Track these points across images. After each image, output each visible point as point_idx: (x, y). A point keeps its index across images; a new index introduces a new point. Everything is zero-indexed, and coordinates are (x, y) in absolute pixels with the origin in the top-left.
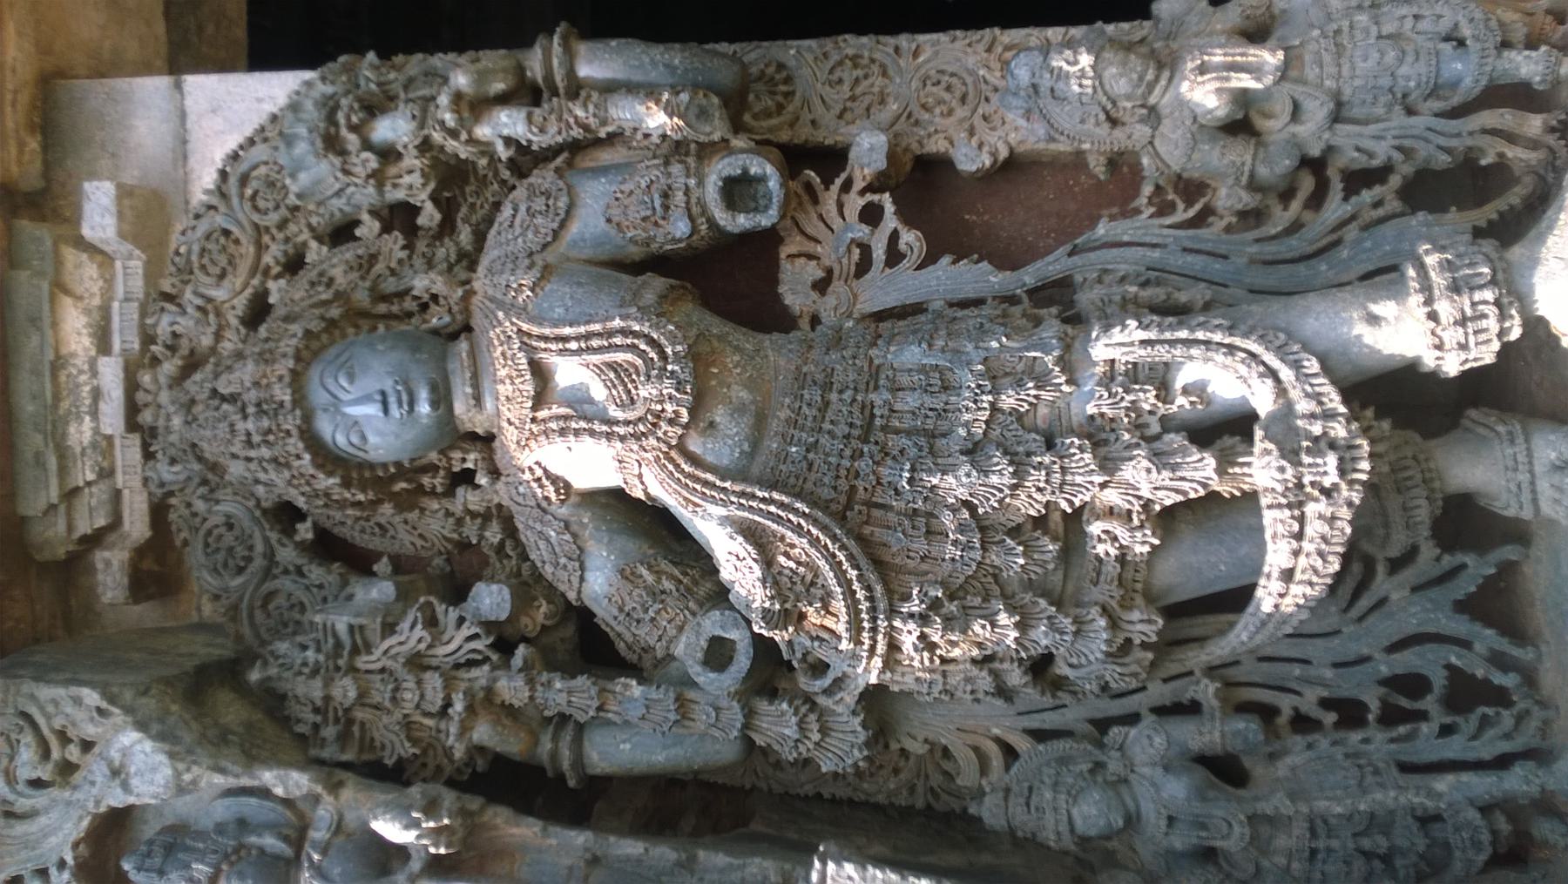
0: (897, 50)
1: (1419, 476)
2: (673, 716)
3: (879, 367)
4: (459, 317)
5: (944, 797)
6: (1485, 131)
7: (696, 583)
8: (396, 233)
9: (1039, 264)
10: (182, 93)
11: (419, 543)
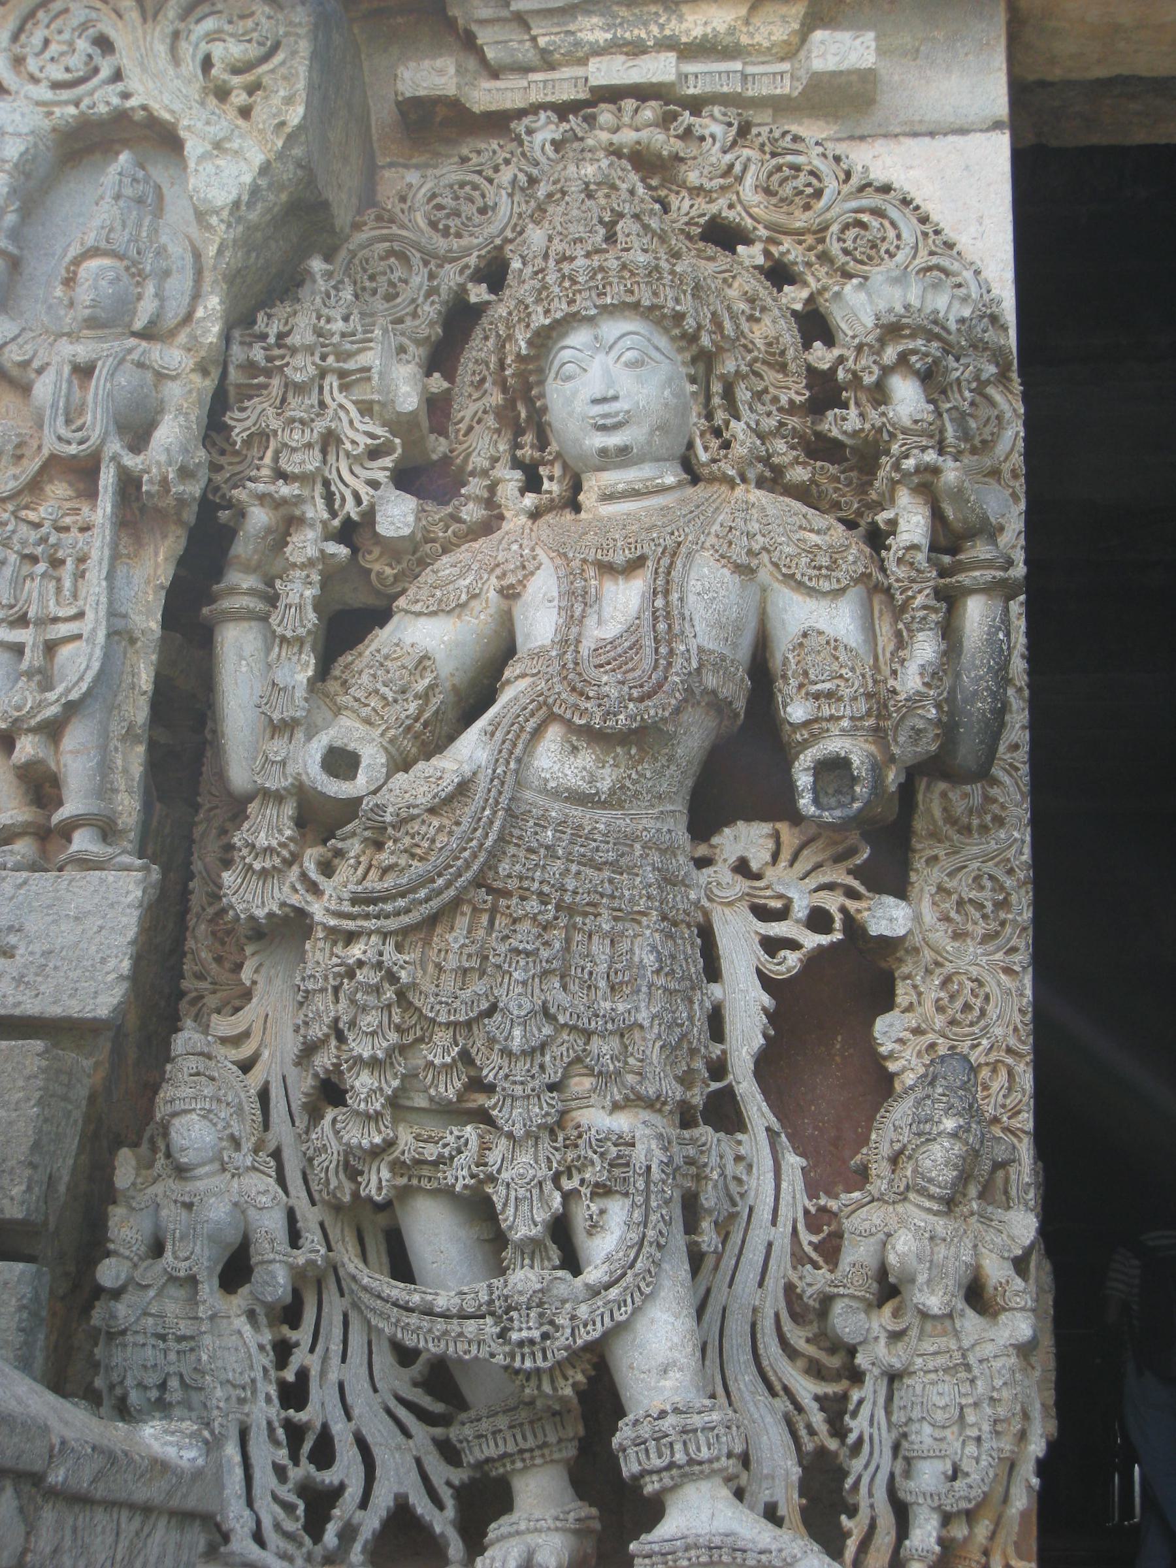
1: (528, 1446)
2: (276, 716)
3: (639, 923)
4: (706, 471)
9: (759, 1097)
10: (987, 130)
11: (463, 426)
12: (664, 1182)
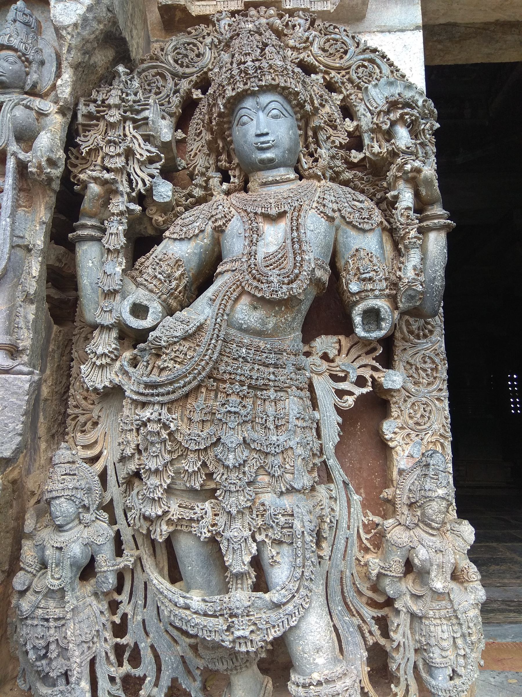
0: (441, 390)
2: (106, 288)
5: (73, 423)
6: (408, 686)
7: (175, 298)
8: (348, 139)
9: (339, 467)
10: (413, 30)
11: (192, 153)
12: (312, 541)
